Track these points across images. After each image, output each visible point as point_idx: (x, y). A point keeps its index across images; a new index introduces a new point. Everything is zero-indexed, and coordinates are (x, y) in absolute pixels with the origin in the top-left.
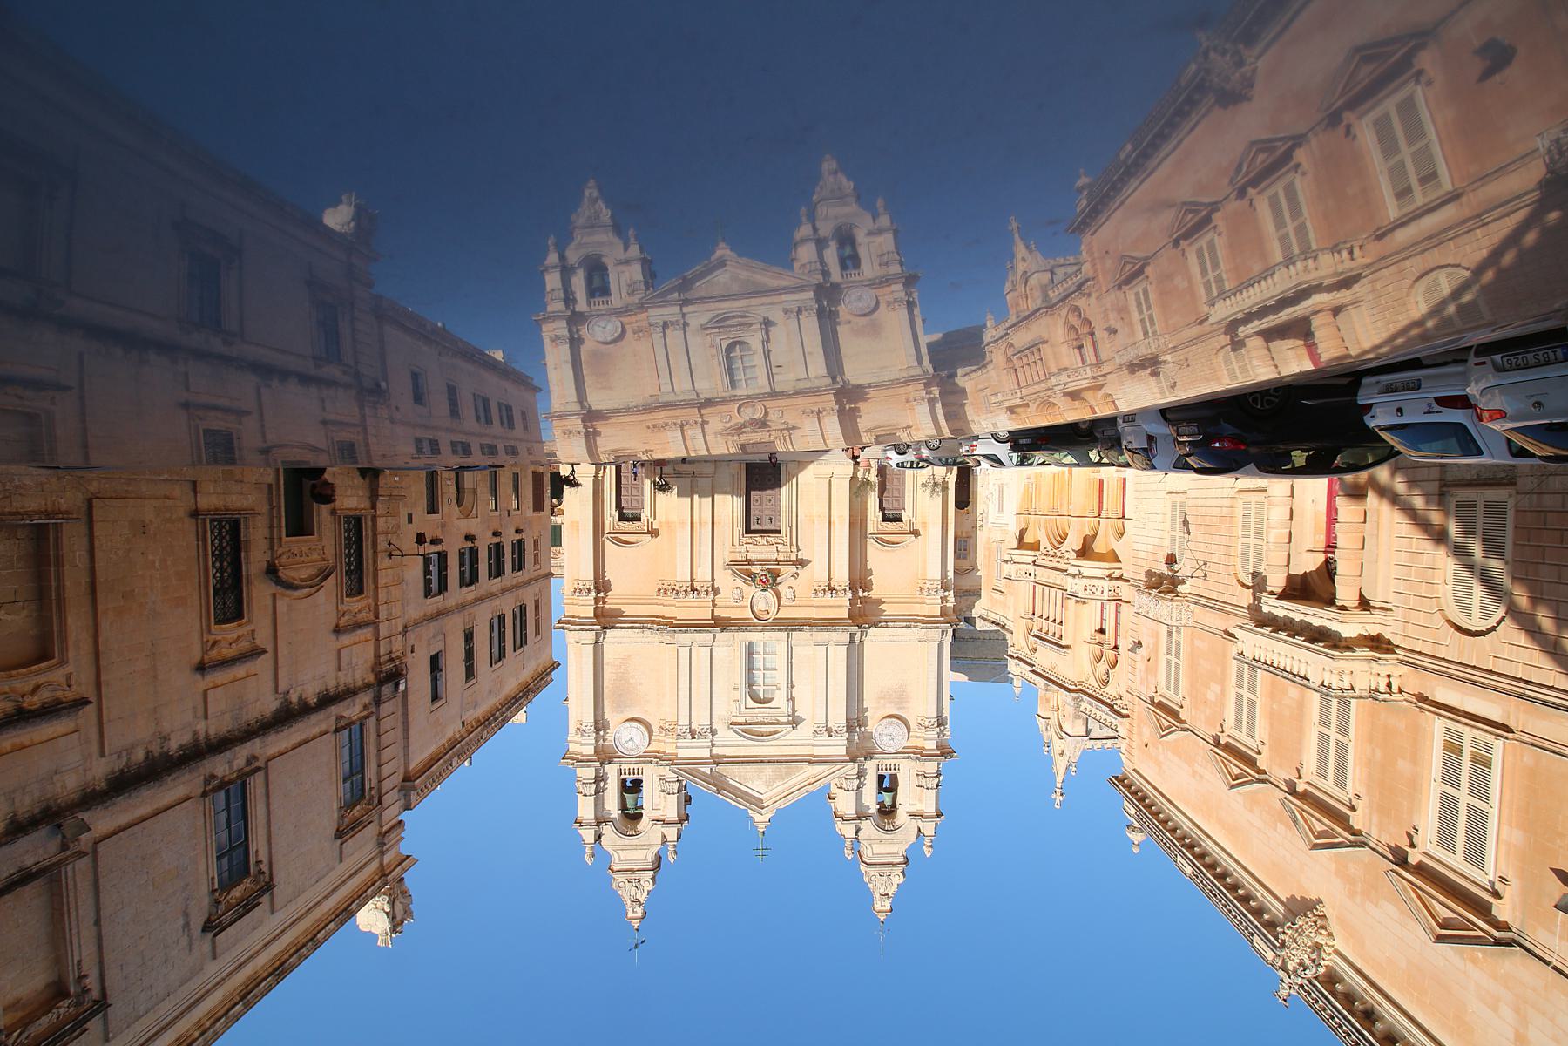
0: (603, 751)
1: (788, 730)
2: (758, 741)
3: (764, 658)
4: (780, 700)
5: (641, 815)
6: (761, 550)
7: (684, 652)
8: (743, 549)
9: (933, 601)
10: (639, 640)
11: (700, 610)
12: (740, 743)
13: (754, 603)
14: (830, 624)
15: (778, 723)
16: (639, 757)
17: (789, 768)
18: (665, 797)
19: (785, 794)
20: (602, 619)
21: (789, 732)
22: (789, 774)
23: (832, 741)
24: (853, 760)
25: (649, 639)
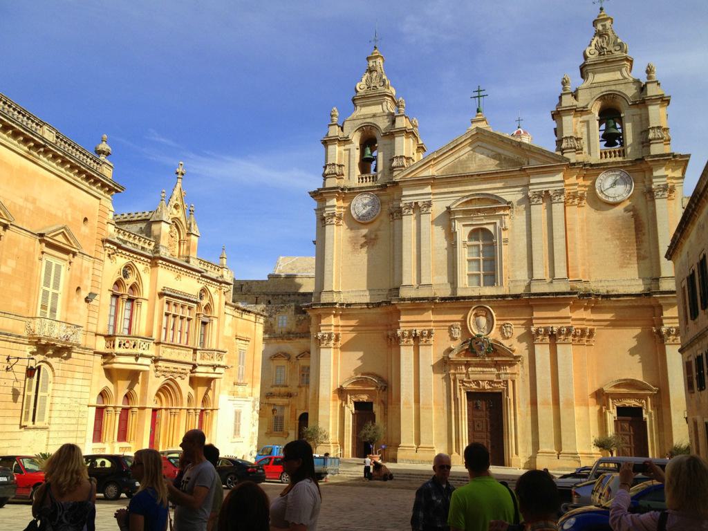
0: (644, 171)
1: (454, 206)
2: (482, 194)
3: (480, 271)
4: (462, 232)
5: (599, 115)
6: (484, 377)
7: (560, 272)
8: (503, 377)
9: (327, 328)
10: (612, 284)
11: (545, 319)
12: (500, 191)
13: (491, 322)
14: (419, 304)
15: (465, 212)
16: (604, 169)
17: (454, 171)
18: (577, 133)
19: (457, 149)
20: (653, 303)
21: (454, 204)
22: (454, 166)
23: (413, 200)
24: (396, 184)
25: (600, 284)
